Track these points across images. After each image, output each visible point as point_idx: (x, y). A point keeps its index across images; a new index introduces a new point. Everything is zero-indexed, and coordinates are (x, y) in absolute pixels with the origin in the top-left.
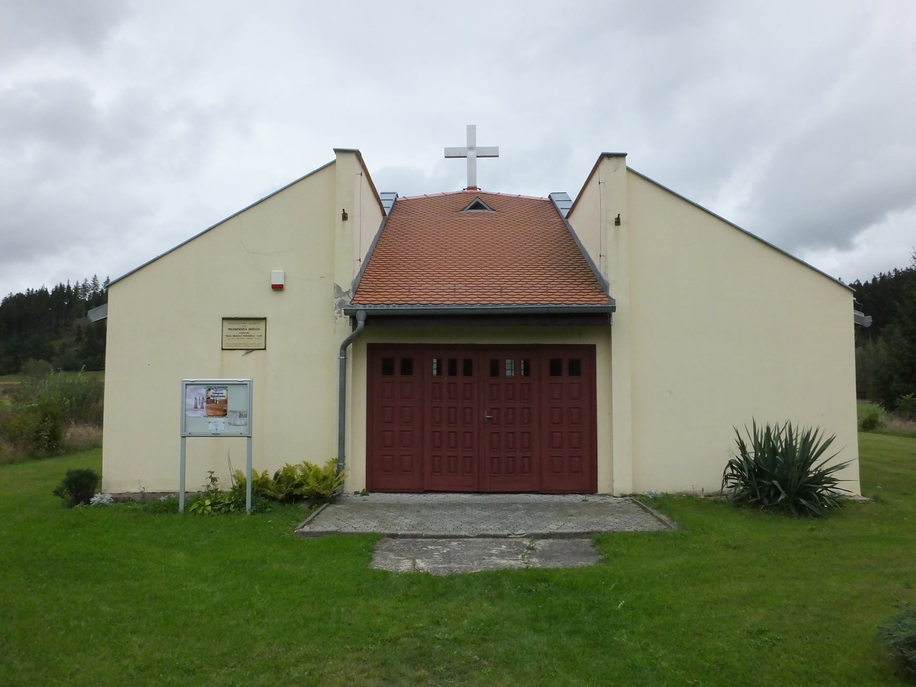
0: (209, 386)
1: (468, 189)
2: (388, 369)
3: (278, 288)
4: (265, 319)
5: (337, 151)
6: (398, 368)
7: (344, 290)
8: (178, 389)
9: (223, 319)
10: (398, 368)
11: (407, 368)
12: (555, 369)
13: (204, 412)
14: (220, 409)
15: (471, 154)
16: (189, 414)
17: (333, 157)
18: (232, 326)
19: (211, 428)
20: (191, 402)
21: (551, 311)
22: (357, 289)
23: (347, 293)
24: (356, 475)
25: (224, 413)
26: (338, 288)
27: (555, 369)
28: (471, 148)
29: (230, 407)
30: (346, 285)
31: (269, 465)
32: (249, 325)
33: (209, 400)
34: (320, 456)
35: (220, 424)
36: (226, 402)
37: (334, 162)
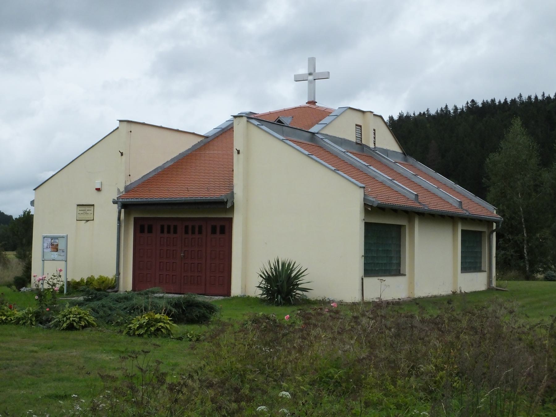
0: (52, 238)
1: (308, 103)
2: (142, 231)
3: (98, 190)
4: (93, 205)
5: (120, 121)
6: (146, 230)
7: (121, 191)
8: (41, 239)
9: (78, 205)
10: (146, 230)
11: (150, 231)
12: (214, 231)
13: (49, 250)
14: (55, 248)
15: (311, 78)
16: (45, 250)
17: (117, 124)
18: (81, 209)
19: (52, 257)
20: (45, 245)
21: (197, 201)
22: (128, 189)
23: (122, 192)
24: (127, 284)
25: (57, 250)
26: (119, 190)
27: (214, 231)
28: (310, 74)
29: (59, 248)
30: (122, 189)
31: (78, 274)
32: (87, 208)
33: (52, 245)
34: (110, 273)
35: (55, 255)
36: (58, 245)
37: (118, 128)
